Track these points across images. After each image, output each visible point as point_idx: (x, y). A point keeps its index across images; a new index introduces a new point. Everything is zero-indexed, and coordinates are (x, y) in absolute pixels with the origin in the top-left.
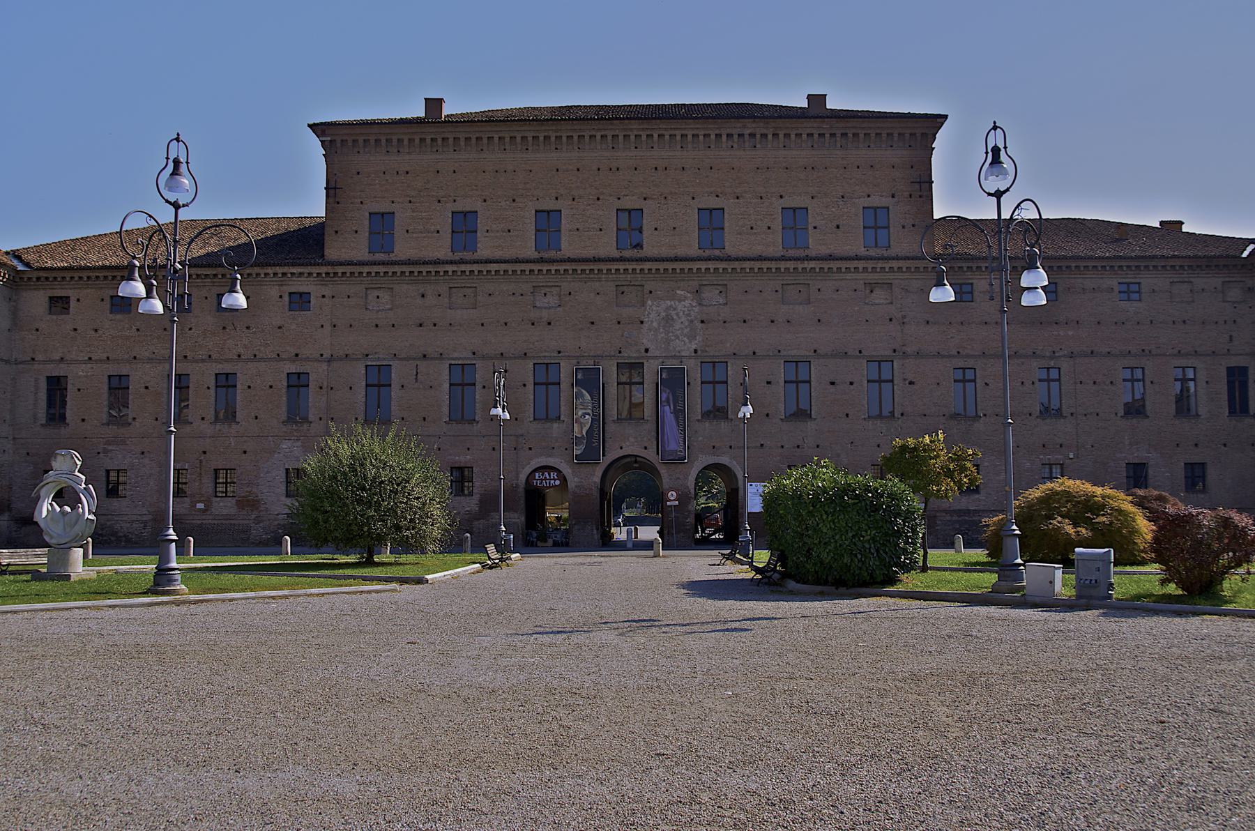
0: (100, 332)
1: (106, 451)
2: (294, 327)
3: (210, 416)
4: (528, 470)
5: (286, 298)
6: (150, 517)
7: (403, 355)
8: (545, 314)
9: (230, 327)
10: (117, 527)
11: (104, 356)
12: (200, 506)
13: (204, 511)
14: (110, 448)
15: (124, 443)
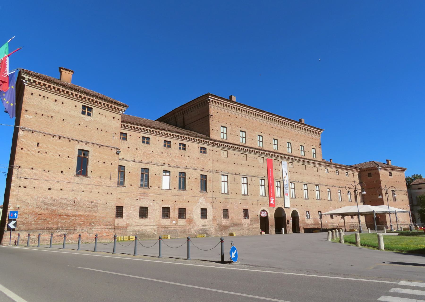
0: (138, 150)
1: (140, 199)
2: (202, 159)
3: (177, 186)
4: (260, 211)
5: (200, 148)
6: (157, 227)
7: (231, 173)
8: (261, 165)
9: (183, 156)
10: (144, 231)
11: (140, 160)
12: (174, 222)
13: (175, 224)
14: (142, 197)
15: (147, 196)
